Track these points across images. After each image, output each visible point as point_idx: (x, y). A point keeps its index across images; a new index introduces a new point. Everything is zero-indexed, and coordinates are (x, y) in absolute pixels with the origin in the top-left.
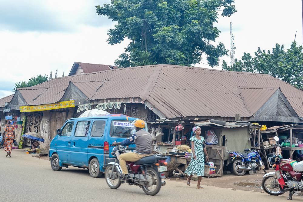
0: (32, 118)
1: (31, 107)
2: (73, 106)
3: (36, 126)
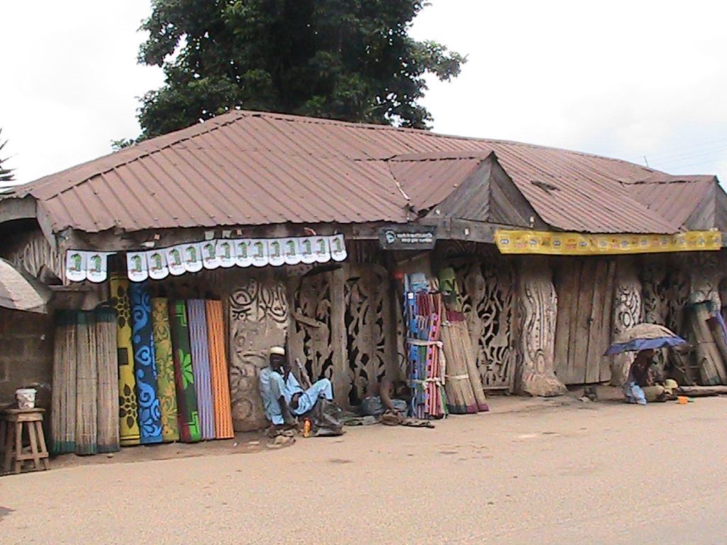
0: (472, 281)
1: (563, 239)
3: (490, 311)
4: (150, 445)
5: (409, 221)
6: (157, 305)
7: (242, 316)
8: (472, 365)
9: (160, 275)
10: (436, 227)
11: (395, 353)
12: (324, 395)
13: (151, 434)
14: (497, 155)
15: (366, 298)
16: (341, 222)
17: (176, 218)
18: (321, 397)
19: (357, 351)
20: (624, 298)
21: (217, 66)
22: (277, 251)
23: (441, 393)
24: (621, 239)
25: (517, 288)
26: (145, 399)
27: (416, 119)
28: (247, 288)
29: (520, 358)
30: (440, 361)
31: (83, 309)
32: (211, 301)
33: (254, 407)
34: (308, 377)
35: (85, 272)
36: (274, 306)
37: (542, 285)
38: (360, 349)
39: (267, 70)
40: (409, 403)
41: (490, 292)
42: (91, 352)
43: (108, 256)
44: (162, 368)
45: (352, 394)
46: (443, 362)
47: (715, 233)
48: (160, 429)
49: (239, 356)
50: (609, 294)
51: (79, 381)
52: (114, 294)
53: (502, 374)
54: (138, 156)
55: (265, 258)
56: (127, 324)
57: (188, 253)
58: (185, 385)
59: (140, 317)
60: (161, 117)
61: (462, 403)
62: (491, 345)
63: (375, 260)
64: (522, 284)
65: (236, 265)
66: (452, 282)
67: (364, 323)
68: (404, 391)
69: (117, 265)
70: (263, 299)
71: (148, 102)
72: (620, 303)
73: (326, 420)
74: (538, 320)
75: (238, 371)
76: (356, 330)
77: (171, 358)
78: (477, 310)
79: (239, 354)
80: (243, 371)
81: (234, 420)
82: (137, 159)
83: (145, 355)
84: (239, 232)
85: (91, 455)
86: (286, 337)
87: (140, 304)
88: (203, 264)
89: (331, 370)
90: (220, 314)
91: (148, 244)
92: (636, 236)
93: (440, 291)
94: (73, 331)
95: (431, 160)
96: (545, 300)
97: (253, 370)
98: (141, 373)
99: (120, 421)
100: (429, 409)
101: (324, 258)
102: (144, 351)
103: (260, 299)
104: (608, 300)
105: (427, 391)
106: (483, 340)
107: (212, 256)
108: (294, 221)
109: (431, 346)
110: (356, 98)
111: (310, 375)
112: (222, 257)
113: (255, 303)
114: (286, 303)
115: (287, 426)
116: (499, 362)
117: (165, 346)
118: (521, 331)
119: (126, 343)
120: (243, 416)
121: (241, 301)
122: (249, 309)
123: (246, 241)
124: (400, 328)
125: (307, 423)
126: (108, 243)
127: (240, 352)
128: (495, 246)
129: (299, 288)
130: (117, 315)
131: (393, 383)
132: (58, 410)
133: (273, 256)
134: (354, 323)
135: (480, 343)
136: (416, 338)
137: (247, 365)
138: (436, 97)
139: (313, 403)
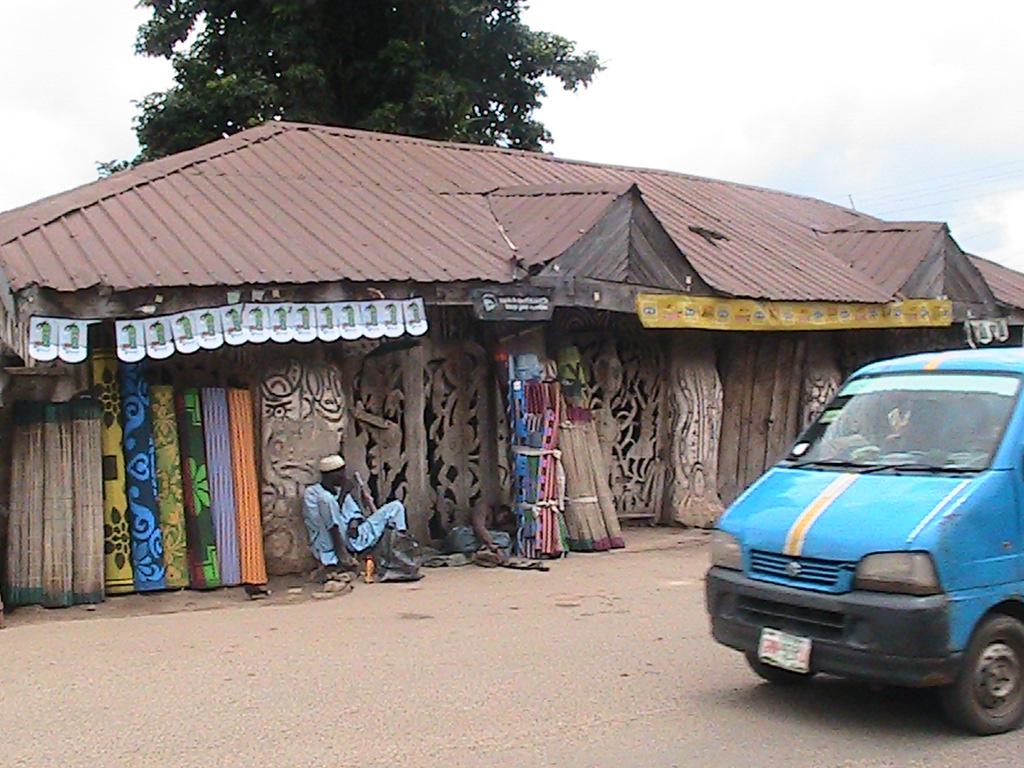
0: (605, 365)
1: (732, 308)
2: (946, 321)
3: (628, 408)
4: (149, 593)
5: (516, 280)
6: (158, 395)
7: (279, 412)
8: (603, 483)
9: (162, 353)
10: (553, 289)
11: (494, 467)
12: (395, 523)
13: (150, 578)
14: (641, 189)
15: (453, 388)
16: (420, 280)
17: (186, 273)
18: (389, 527)
19: (441, 462)
20: (816, 392)
21: (247, 59)
22: (330, 320)
23: (559, 522)
24: (812, 309)
25: (667, 379)
26: (142, 528)
27: (529, 138)
28: (287, 373)
29: (670, 475)
30: (558, 478)
31: (54, 400)
32: (236, 391)
33: (295, 542)
34: (371, 499)
35: (56, 347)
36: (325, 398)
37: (701, 370)
38: (444, 459)
39: (319, 65)
40: (513, 536)
41: (629, 382)
42: (65, 459)
43: (89, 326)
44: (165, 484)
45: (434, 523)
46: (562, 479)
47: (943, 302)
48: (163, 570)
49: (274, 469)
50: (796, 386)
51: (48, 504)
52: (98, 379)
53: (644, 497)
54: (133, 184)
55: (313, 330)
56: (115, 422)
57: (203, 322)
58: (198, 509)
59: (134, 413)
60: (168, 130)
61: (588, 537)
62: (629, 456)
63: (468, 333)
64: (674, 371)
65: (270, 339)
66: (575, 367)
67: (451, 424)
68: (507, 519)
69: (102, 339)
70: (309, 387)
71: (150, 108)
72: (811, 399)
73: (396, 560)
74: (697, 422)
75: (271, 489)
76: (440, 432)
77: (178, 471)
78: (611, 406)
79: (275, 466)
80: (280, 489)
81: (269, 560)
82: (131, 189)
83: (142, 467)
84: (276, 293)
85: (64, 607)
86: (341, 443)
87: (135, 395)
88: (224, 338)
89: (404, 488)
90: (248, 408)
91: (147, 309)
92: (835, 306)
93: (559, 378)
94: (39, 432)
95: (548, 195)
96: (705, 393)
97: (293, 487)
98: (135, 492)
99: (105, 559)
100: (541, 545)
101: (396, 332)
102: (138, 461)
103: (305, 388)
104: (794, 394)
105: (538, 520)
106: (619, 448)
107: (237, 328)
108: (353, 279)
109: (545, 456)
110: (443, 107)
111: (376, 497)
112: (252, 328)
113: (297, 393)
114: (342, 395)
115: (340, 567)
116: (641, 480)
117: (170, 454)
118: (671, 436)
119: (115, 449)
120: (279, 553)
121: (278, 390)
122: (290, 402)
123: (286, 306)
124: (502, 431)
125: (369, 562)
126: (89, 308)
127: (276, 462)
128: (635, 316)
129: (360, 374)
130: (102, 409)
131: (493, 508)
132: (17, 543)
133: (323, 327)
134: (437, 422)
135: (615, 452)
136: (525, 445)
137: (284, 482)
138: (555, 106)
139: (378, 534)
